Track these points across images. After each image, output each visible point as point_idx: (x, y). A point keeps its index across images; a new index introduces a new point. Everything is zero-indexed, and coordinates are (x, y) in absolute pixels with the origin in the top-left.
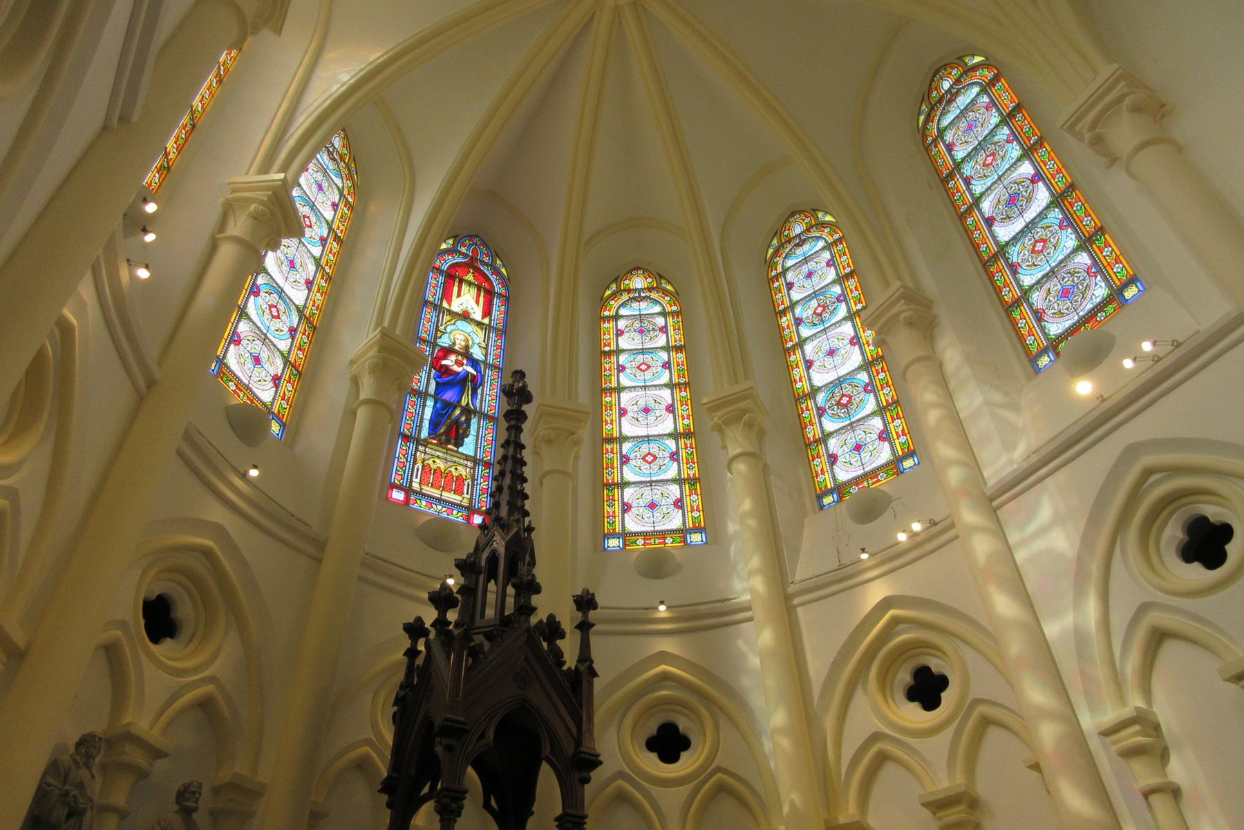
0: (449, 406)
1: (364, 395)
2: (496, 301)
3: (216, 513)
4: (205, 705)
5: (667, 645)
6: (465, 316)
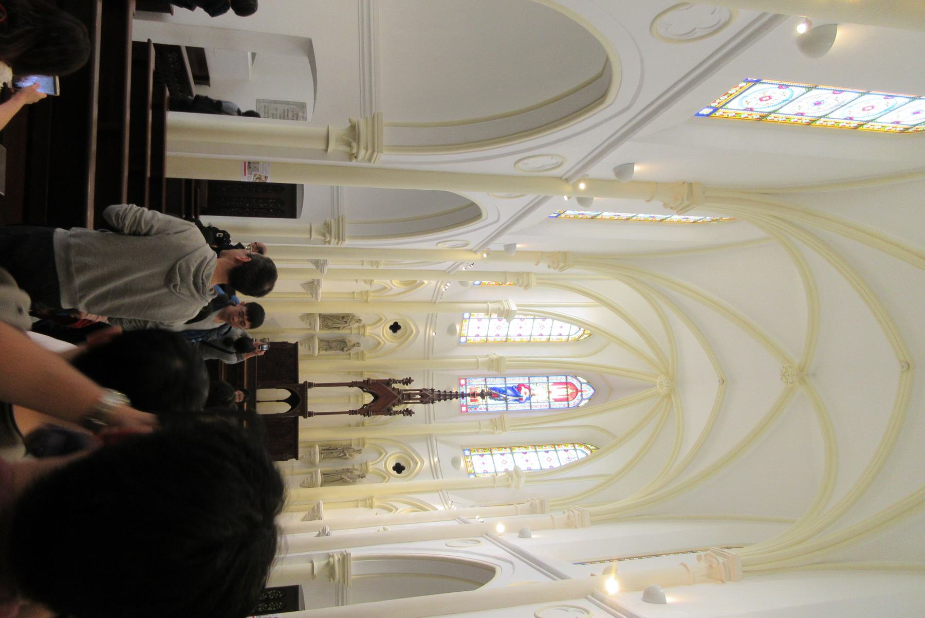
0: (505, 392)
1: (480, 360)
2: (566, 403)
3: (422, 330)
4: (379, 343)
5: (426, 463)
6: (549, 392)
